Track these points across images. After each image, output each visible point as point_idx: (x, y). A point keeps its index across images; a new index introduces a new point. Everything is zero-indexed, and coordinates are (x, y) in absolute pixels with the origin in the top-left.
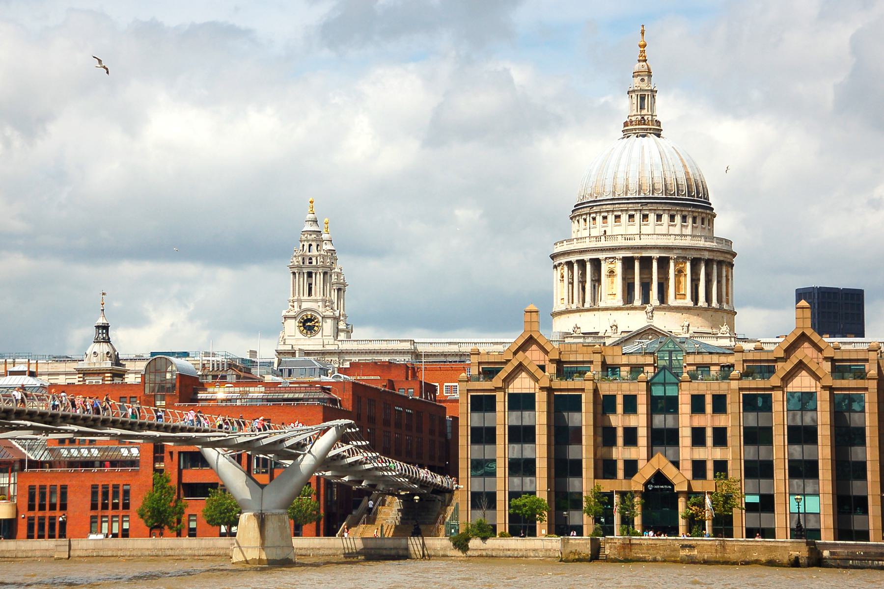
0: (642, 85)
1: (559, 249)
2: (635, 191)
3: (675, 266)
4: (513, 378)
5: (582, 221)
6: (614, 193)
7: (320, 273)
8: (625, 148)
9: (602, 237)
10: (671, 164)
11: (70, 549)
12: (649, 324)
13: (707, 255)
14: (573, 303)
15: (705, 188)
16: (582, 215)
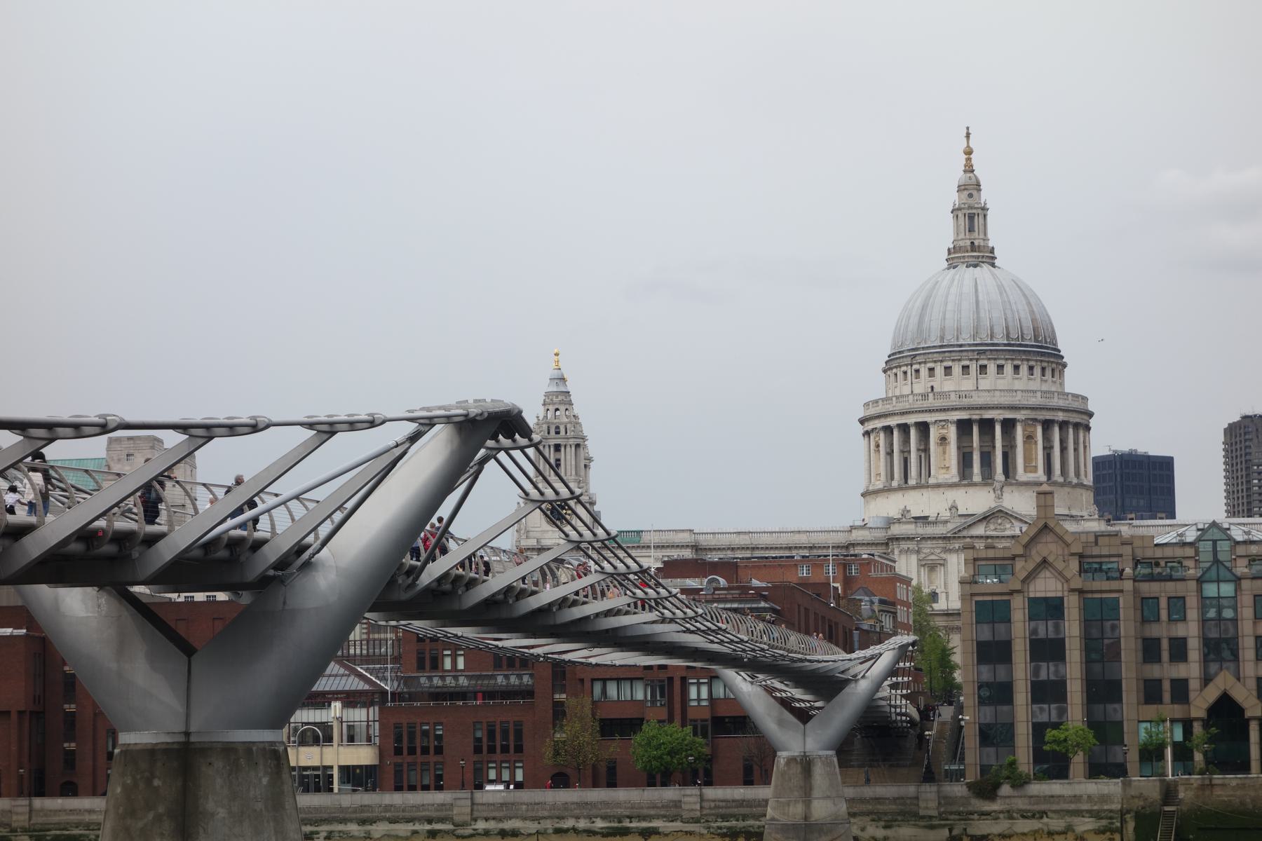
0: (969, 202)
1: (873, 411)
2: (969, 335)
3: (1024, 430)
4: (1034, 578)
5: (900, 375)
6: (942, 338)
7: (571, 446)
8: (953, 280)
9: (929, 394)
10: (1012, 302)
11: (473, 804)
12: (998, 504)
13: (1061, 416)
14: (892, 478)
15: (1053, 331)
16: (900, 367)
